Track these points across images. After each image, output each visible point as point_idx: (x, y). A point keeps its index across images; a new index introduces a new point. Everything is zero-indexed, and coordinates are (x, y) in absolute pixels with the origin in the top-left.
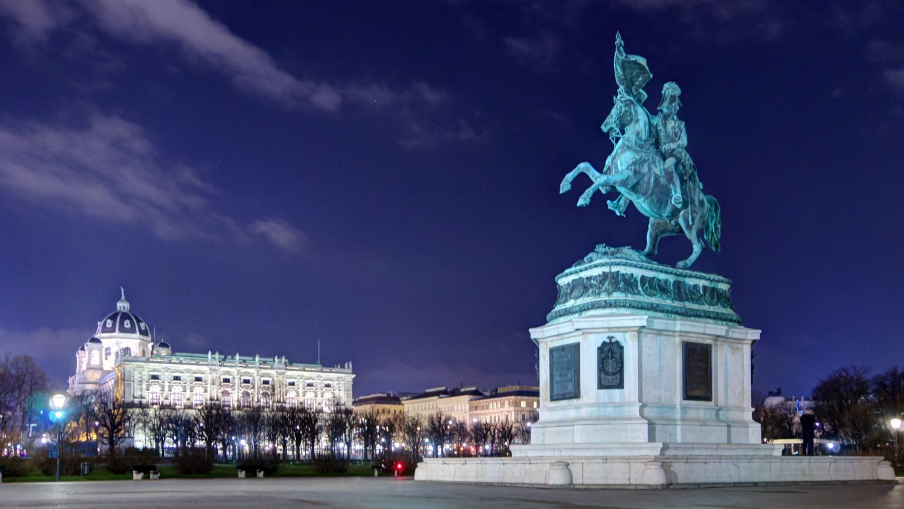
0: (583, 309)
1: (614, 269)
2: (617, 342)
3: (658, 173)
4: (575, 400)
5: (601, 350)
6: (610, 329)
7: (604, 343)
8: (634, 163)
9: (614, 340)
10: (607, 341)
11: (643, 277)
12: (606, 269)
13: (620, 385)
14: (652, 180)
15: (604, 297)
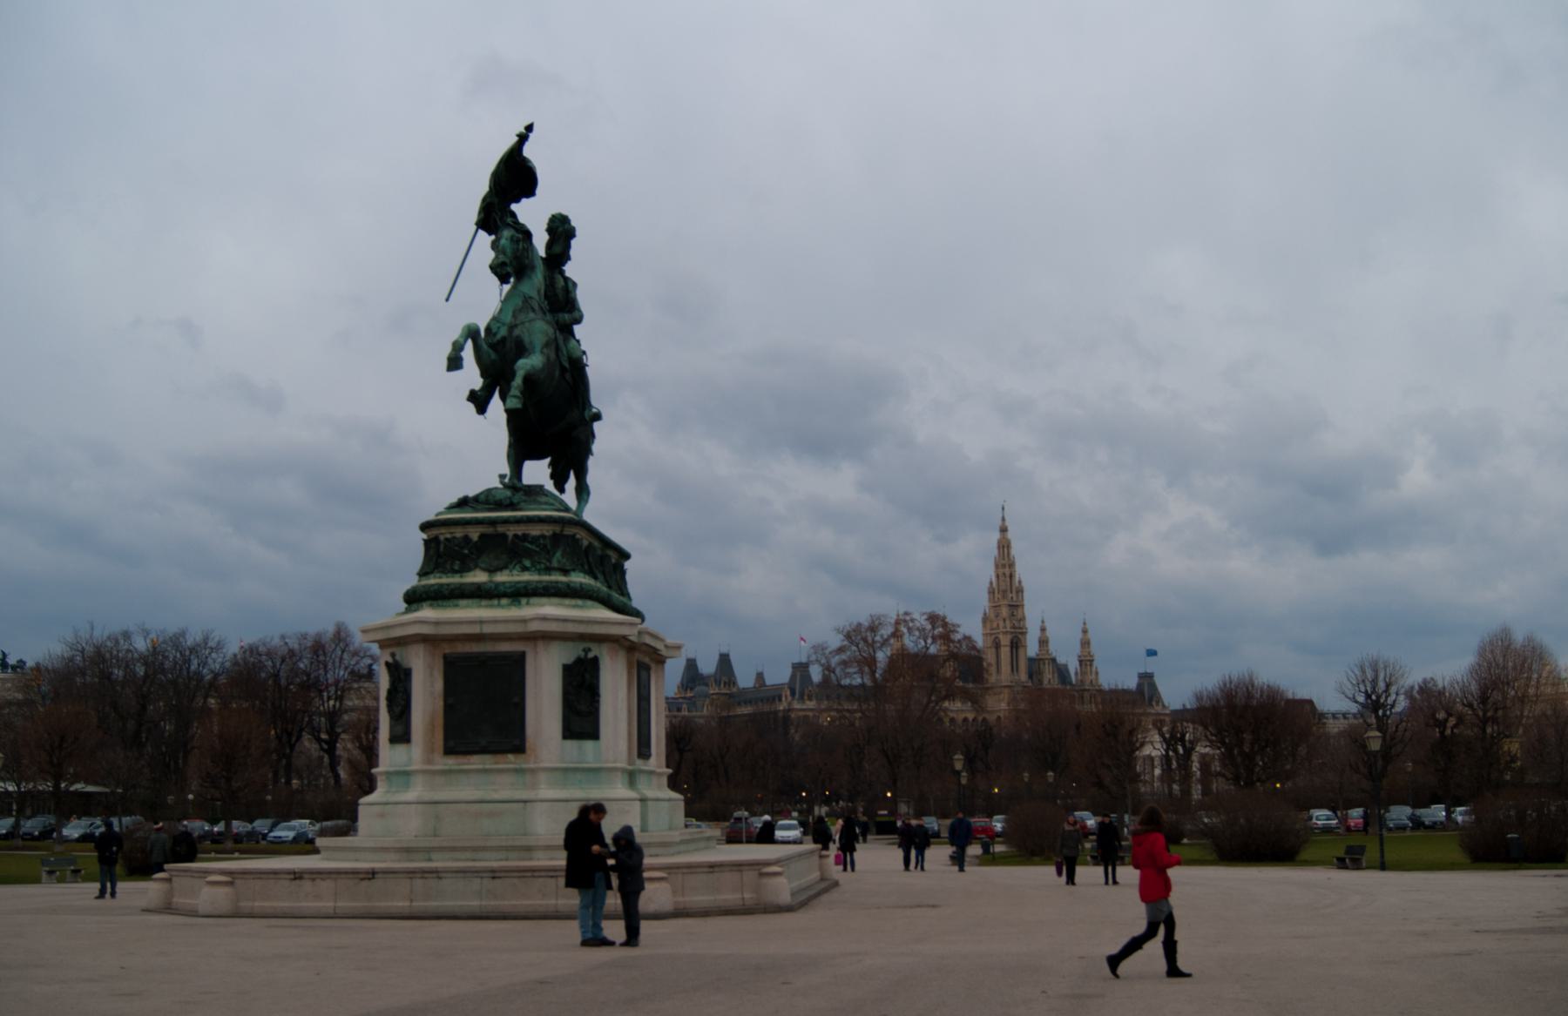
0: (518, 594)
1: (569, 531)
2: (595, 660)
3: (566, 365)
4: (511, 757)
5: (567, 669)
6: (582, 637)
7: (579, 661)
8: (547, 345)
9: (591, 655)
10: (582, 654)
11: (590, 545)
12: (557, 529)
13: (594, 735)
14: (557, 373)
15: (557, 577)
